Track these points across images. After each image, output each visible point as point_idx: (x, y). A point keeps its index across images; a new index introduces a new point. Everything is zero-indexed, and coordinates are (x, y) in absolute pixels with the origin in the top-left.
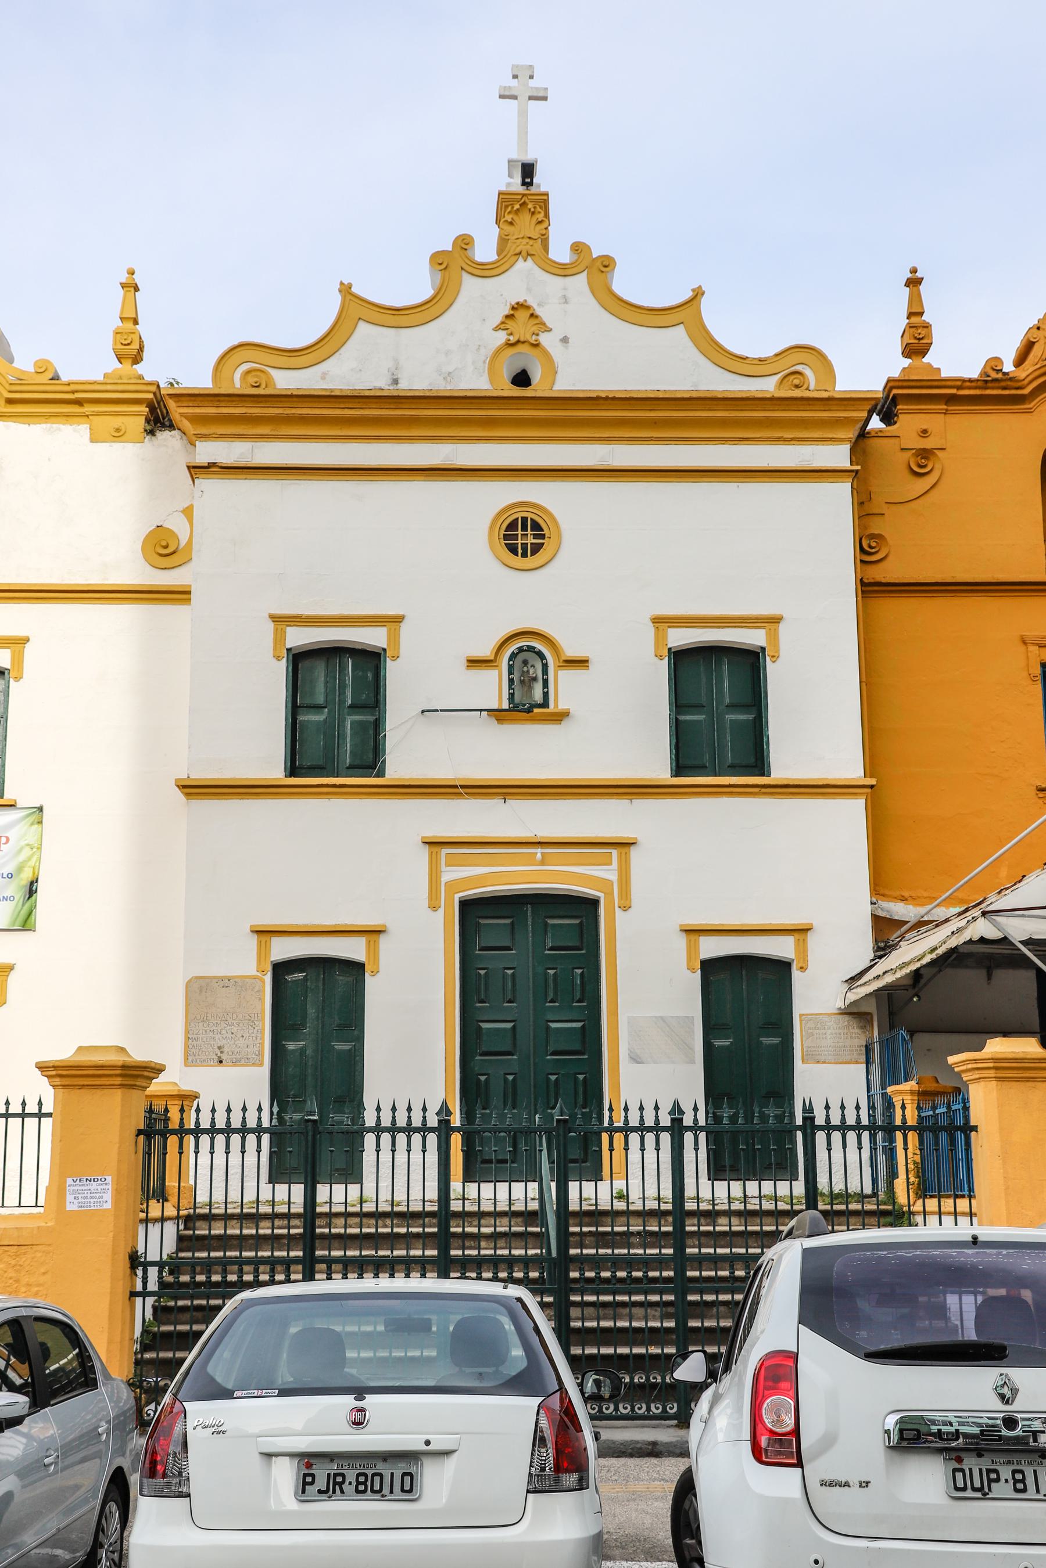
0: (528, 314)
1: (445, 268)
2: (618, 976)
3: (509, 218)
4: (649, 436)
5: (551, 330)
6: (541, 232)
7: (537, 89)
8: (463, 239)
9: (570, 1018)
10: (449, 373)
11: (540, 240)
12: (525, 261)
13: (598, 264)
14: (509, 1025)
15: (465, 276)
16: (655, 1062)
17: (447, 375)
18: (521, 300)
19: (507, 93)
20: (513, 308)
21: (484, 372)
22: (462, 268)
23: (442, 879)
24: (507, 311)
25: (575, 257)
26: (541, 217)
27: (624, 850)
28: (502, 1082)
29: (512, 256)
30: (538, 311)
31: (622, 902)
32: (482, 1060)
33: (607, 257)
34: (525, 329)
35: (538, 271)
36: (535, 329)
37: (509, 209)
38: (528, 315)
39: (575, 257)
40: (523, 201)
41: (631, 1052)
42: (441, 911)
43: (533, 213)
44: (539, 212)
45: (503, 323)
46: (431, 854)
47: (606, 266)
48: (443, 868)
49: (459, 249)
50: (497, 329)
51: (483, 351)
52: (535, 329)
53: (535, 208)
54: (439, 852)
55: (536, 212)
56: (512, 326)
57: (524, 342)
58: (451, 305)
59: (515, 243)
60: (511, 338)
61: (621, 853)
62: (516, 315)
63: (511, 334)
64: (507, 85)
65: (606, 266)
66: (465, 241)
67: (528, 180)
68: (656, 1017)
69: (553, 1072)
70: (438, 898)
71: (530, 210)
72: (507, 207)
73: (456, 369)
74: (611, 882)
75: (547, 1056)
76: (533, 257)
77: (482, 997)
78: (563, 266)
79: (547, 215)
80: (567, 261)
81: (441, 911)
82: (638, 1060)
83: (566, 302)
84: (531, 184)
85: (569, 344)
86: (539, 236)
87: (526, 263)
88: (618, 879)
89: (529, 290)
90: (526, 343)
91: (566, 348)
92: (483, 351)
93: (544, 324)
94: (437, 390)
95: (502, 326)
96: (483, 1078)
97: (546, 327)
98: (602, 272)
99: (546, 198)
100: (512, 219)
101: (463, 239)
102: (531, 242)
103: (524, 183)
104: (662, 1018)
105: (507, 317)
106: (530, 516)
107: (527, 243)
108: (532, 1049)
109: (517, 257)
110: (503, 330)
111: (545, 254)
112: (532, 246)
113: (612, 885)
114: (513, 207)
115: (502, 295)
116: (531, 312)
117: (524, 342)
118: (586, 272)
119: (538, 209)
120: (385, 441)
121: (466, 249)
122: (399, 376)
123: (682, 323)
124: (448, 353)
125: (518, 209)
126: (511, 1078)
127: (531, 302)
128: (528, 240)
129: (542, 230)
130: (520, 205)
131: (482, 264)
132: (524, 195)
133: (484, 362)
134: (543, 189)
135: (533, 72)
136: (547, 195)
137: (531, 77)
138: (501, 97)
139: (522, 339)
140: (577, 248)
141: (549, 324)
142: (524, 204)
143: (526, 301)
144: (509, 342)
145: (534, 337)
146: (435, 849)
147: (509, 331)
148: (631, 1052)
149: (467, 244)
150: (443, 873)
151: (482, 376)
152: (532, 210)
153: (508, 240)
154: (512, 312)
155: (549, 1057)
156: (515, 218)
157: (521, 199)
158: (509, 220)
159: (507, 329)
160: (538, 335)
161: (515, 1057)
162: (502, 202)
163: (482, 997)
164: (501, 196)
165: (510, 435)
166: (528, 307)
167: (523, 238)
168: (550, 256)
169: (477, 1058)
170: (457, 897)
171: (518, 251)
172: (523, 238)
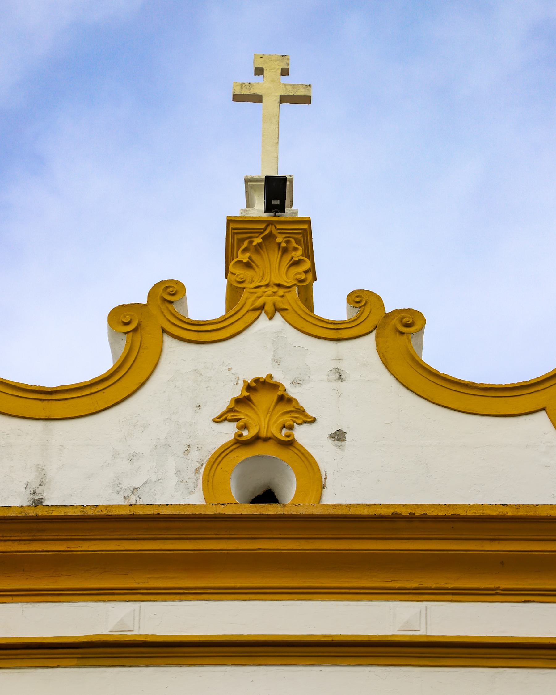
0: (272, 397)
1: (135, 330)
3: (244, 258)
4: (492, 586)
5: (314, 421)
6: (298, 277)
7: (293, 86)
8: (167, 287)
10: (135, 489)
11: (296, 289)
12: (271, 318)
13: (395, 321)
15: (168, 340)
17: (130, 492)
18: (263, 376)
19: (245, 92)
20: (249, 388)
21: (195, 487)
22: (164, 331)
24: (238, 391)
25: (355, 312)
26: (298, 255)
29: (248, 311)
30: (292, 392)
33: (410, 311)
34: (269, 421)
35: (292, 334)
36: (287, 419)
38: (275, 398)
39: (355, 312)
43: (285, 251)
44: (295, 249)
45: (230, 410)
47: (408, 325)
49: (159, 302)
50: (219, 420)
51: (195, 454)
52: (287, 419)
53: (288, 242)
55: (290, 249)
56: (246, 415)
57: (266, 440)
58: (143, 385)
59: (255, 293)
60: (245, 433)
62: (253, 398)
63: (245, 427)
64: (246, 81)
65: (408, 325)
67: (276, 202)
71: (279, 244)
72: (241, 241)
73: (146, 483)
76: (284, 313)
78: (336, 326)
79: (309, 253)
83: (340, 379)
84: (281, 209)
85: (346, 443)
86: (295, 282)
87: (272, 322)
89: (277, 361)
90: (271, 441)
91: (341, 448)
92: (195, 454)
93: (302, 411)
94: (107, 506)
95: (229, 416)
97: (306, 416)
98: (402, 333)
99: (305, 226)
100: (250, 258)
101: (167, 287)
102: (281, 292)
103: (269, 208)
105: (238, 401)
107: (275, 293)
109: (258, 313)
110: (231, 421)
111: (307, 311)
112: (282, 296)
114: (251, 242)
115: (230, 369)
116: (280, 393)
117: (266, 440)
118: (374, 334)
119: (294, 244)
120: (9, 599)
121: (171, 302)
122: (45, 495)
123: (544, 409)
124: (132, 458)
125: (259, 245)
127: (278, 378)
128: (276, 289)
129: (300, 273)
130: (262, 238)
131: (199, 324)
132: (269, 223)
133: (197, 471)
134: (301, 215)
135: (288, 64)
136: (308, 222)
137: (285, 72)
138: (237, 98)
139: (263, 434)
140: (358, 299)
141: (311, 412)
142: (270, 237)
143: (271, 376)
144: (242, 439)
145: (284, 431)
147: (241, 423)
149: (174, 295)
151: (192, 493)
152: (283, 245)
153: (244, 288)
154: (247, 394)
156: (254, 257)
157: (265, 229)
158: (245, 261)
159: (238, 420)
160: (291, 428)
164: (232, 225)
165: (239, 585)
166: (275, 386)
167: (267, 285)
171: (259, 303)
172: (267, 285)
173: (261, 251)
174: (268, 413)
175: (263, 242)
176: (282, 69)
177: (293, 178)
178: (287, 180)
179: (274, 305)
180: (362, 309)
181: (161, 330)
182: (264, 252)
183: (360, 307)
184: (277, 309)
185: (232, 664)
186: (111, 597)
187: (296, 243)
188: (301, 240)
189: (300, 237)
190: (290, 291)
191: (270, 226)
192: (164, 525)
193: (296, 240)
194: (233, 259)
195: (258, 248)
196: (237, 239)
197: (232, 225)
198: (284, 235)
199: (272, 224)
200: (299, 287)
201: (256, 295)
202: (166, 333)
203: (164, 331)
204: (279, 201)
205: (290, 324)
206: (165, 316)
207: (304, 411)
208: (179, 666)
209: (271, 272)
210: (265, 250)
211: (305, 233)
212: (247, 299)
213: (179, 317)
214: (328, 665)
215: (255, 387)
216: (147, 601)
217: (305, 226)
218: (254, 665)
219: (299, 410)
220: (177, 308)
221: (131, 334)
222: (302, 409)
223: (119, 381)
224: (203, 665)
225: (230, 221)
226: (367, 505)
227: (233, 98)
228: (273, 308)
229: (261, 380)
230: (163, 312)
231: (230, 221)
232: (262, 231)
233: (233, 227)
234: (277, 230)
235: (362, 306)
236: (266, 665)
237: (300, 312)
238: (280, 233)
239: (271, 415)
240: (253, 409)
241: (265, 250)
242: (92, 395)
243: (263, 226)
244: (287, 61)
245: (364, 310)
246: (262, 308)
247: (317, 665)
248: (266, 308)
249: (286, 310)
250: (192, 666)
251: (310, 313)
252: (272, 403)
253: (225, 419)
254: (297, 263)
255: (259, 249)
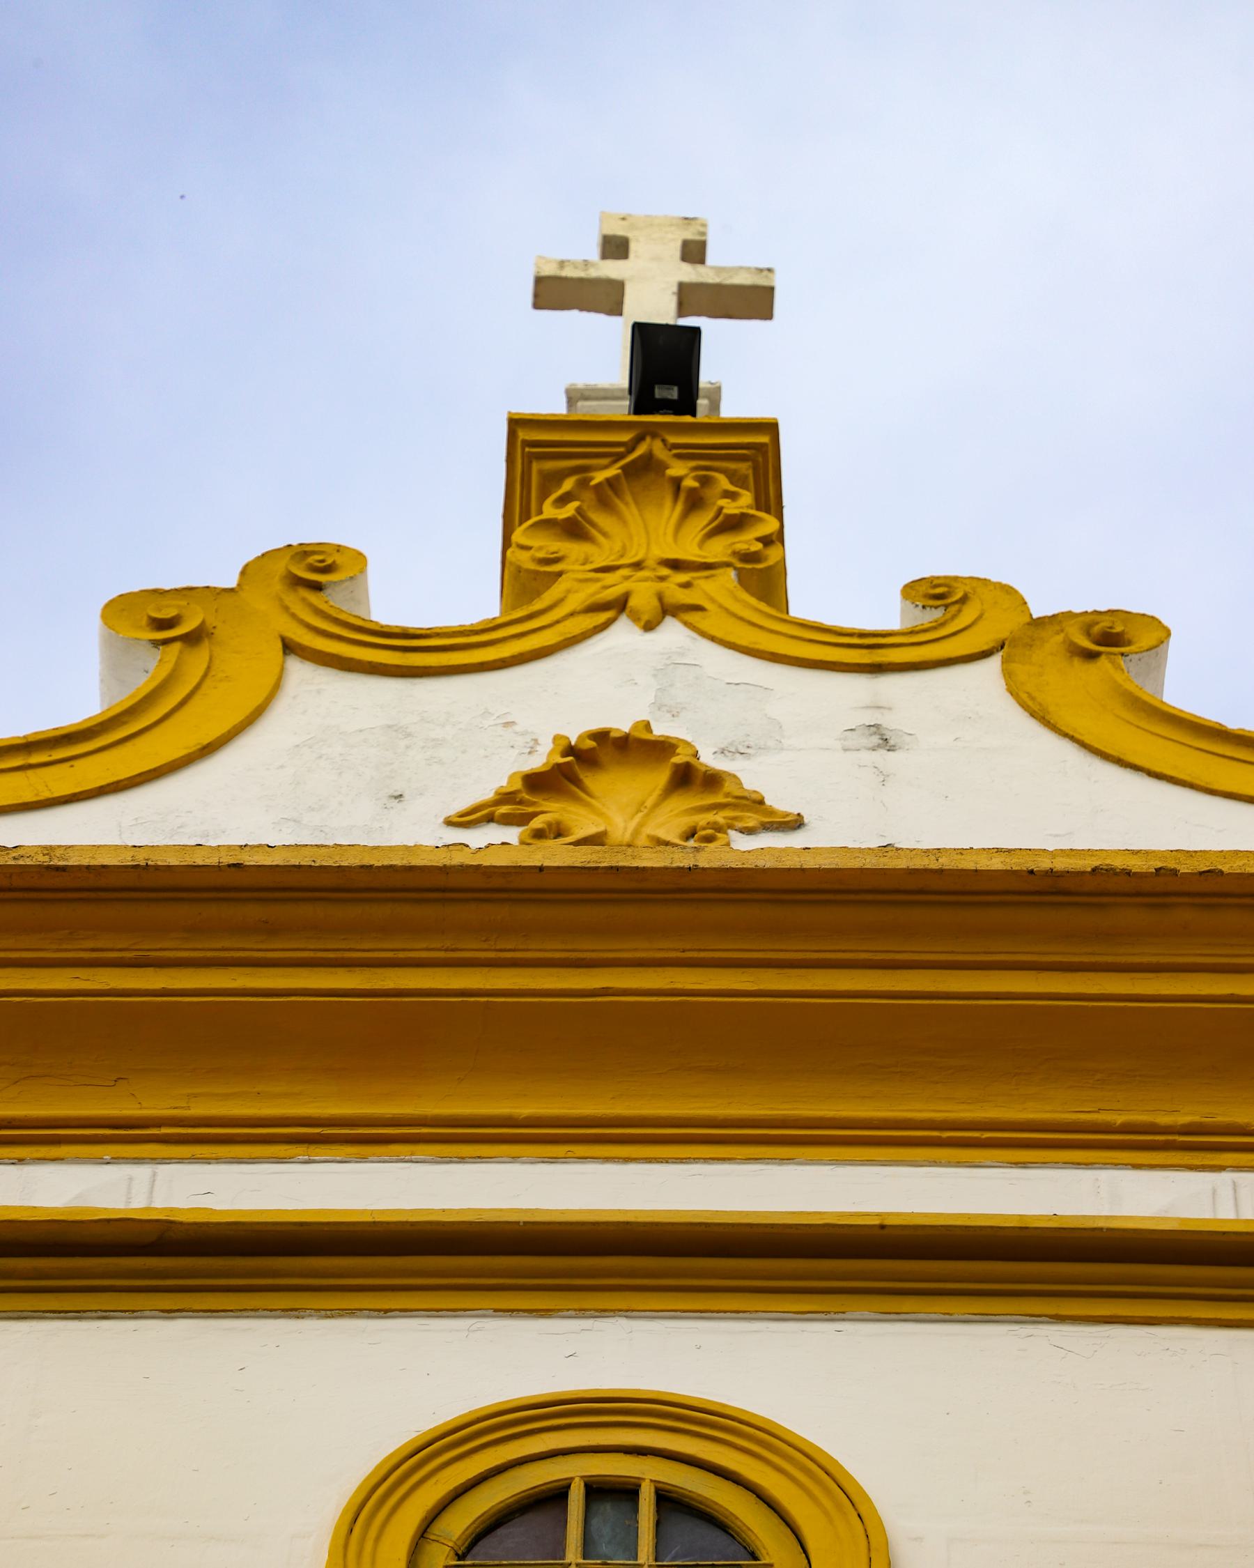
22: (289, 647)
37: (568, 485)
40: (641, 450)
43: (694, 502)
45: (505, 797)
49: (277, 586)
53: (705, 481)
58: (207, 750)
66: (312, 559)
71: (677, 482)
72: (556, 478)
76: (693, 617)
80: (894, 624)
83: (886, 743)
84: (687, 404)
99: (764, 439)
105: (536, 782)
106: (649, 1473)
110: (507, 821)
118: (995, 662)
119: (724, 483)
125: (610, 482)
130: (622, 468)
135: (704, 234)
136: (771, 428)
149: (328, 569)
152: (689, 483)
157: (631, 447)
162: (529, 459)
164: (523, 435)
166: (663, 748)
168: (798, 610)
172: (638, 566)
173: (617, 501)
174: (639, 811)
175: (623, 480)
176: (686, 245)
177: (719, 389)
178: (701, 393)
179: (660, 598)
180: (953, 609)
181: (280, 645)
182: (627, 504)
183: (946, 606)
184: (668, 610)
185: (496, 1310)
186: (43, 1151)
187: (732, 483)
188: (746, 477)
189: (744, 468)
190: (713, 576)
191: (648, 439)
192: (254, 912)
193: (732, 477)
194: (528, 518)
195: (606, 496)
196: (540, 472)
197: (523, 435)
198: (693, 464)
199: (654, 436)
200: (739, 572)
201: (599, 585)
202: (296, 654)
203: (289, 647)
204: (676, 389)
205: (713, 639)
206: (294, 616)
207: (761, 802)
208: (290, 1317)
209: (648, 544)
210: (629, 498)
211: (760, 459)
212: (568, 591)
213: (342, 617)
214: (867, 1314)
215: (592, 749)
216: (181, 1160)
217: (764, 439)
218: (581, 1313)
219: (745, 802)
220: (335, 601)
221: (177, 646)
222: (754, 796)
223: (129, 745)
224: (386, 1311)
225: (516, 424)
226: (999, 850)
227: (536, 295)
228: (655, 603)
229: (613, 735)
230: (286, 609)
231: (516, 424)
232: (621, 449)
233: (527, 438)
234: (670, 450)
235: (956, 602)
236: (628, 1313)
237: (747, 614)
238: (679, 456)
239: (647, 815)
240: (588, 805)
241: (629, 498)
242: (30, 773)
243: (625, 437)
244: (702, 229)
245: (959, 611)
246: (620, 605)
247: (822, 1316)
248: (632, 603)
249: (698, 608)
250: (341, 1316)
251: (784, 616)
252: (654, 790)
253: (490, 819)
254: (734, 524)
255: (610, 493)
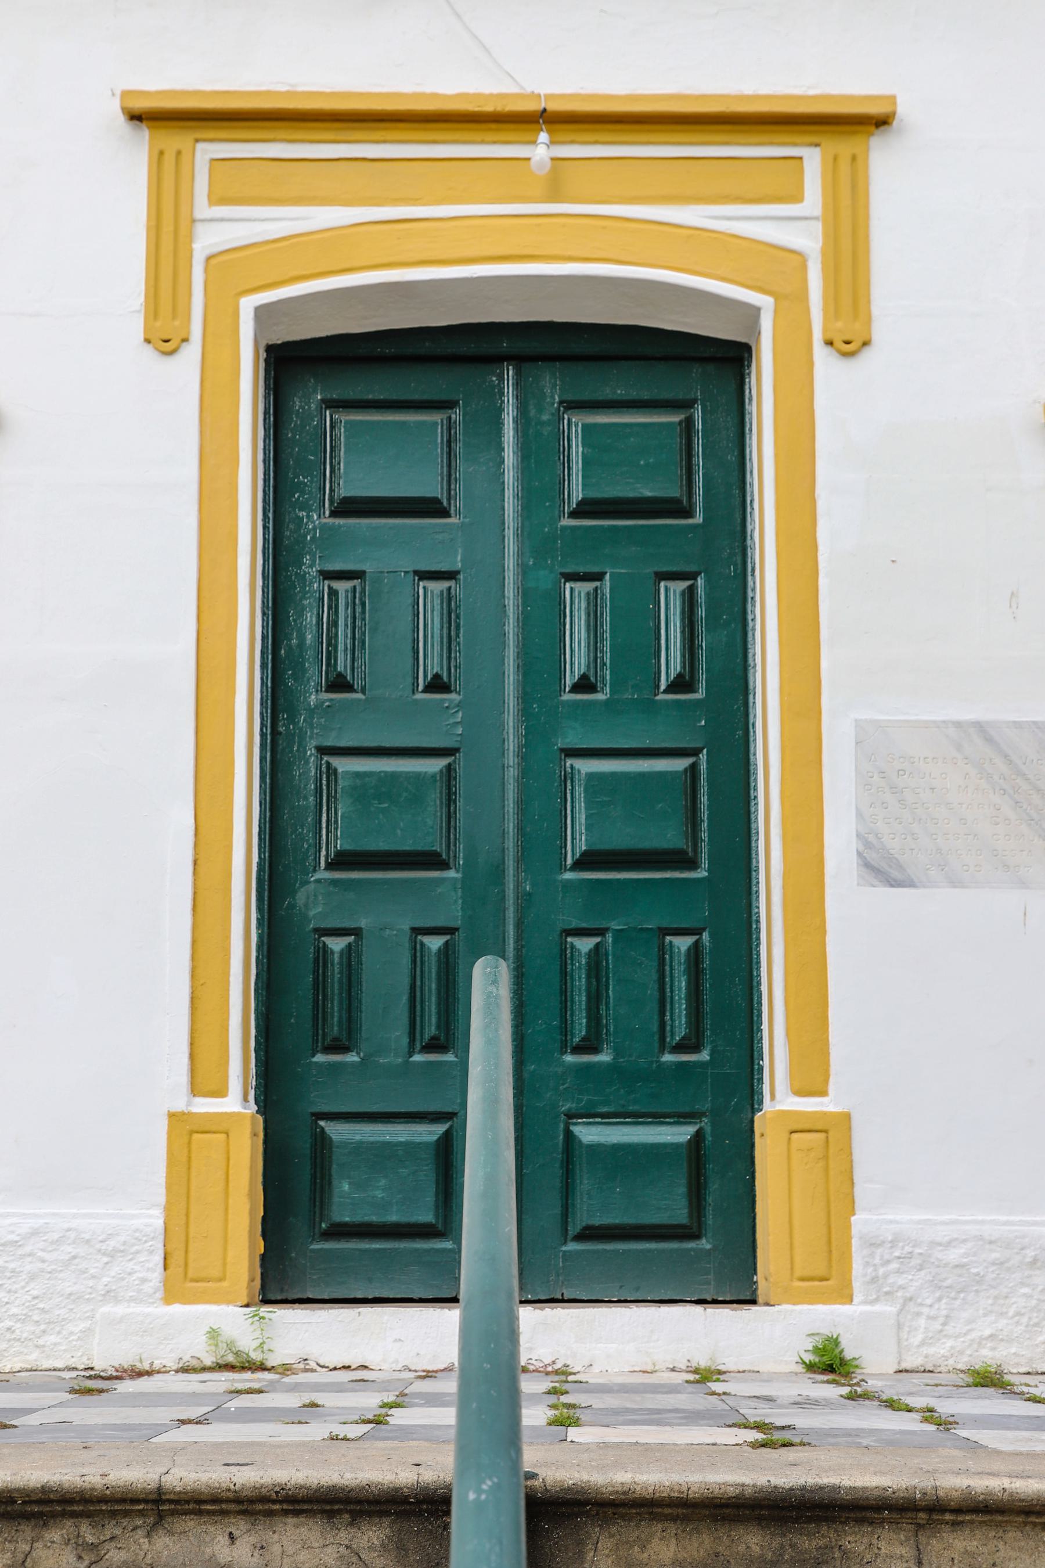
2: (823, 581)
9: (647, 743)
14: (434, 766)
16: (955, 883)
23: (197, 246)
27: (844, 146)
28: (406, 960)
31: (839, 324)
32: (334, 882)
41: (868, 845)
42: (192, 353)
46: (158, 159)
48: (202, 208)
54: (185, 158)
61: (835, 158)
68: (958, 725)
69: (584, 925)
70: (180, 309)
74: (800, 257)
75: (563, 868)
77: (340, 668)
81: (192, 353)
82: (895, 874)
88: (824, 252)
96: (337, 944)
104: (980, 727)
108: (510, 844)
113: (804, 267)
126: (435, 943)
146: (175, 140)
148: (868, 845)
150: (200, 229)
155: (568, 876)
161: (452, 874)
163: (340, 668)
169: (318, 876)
170: (248, 305)
